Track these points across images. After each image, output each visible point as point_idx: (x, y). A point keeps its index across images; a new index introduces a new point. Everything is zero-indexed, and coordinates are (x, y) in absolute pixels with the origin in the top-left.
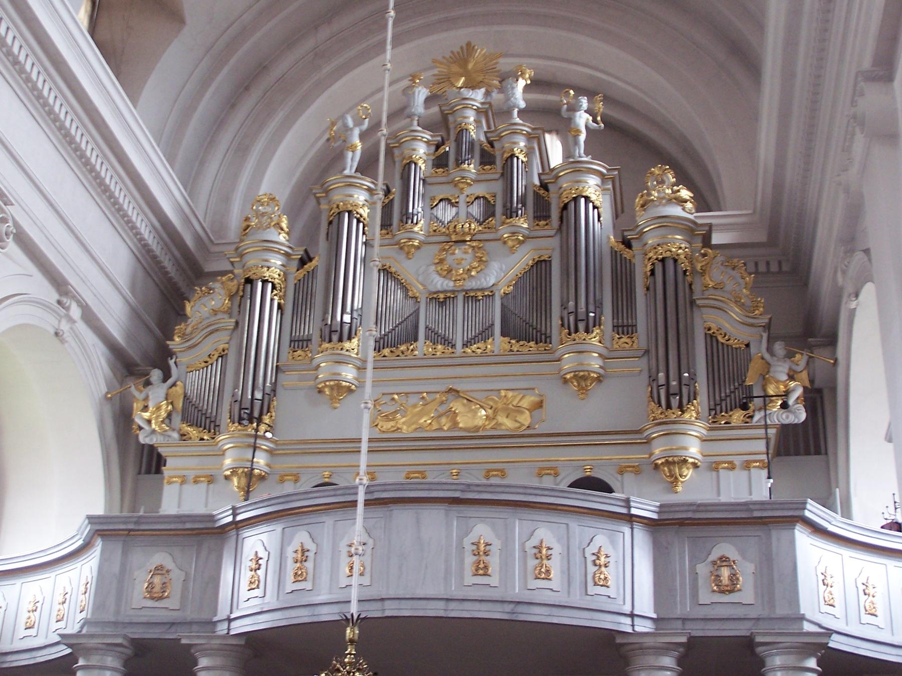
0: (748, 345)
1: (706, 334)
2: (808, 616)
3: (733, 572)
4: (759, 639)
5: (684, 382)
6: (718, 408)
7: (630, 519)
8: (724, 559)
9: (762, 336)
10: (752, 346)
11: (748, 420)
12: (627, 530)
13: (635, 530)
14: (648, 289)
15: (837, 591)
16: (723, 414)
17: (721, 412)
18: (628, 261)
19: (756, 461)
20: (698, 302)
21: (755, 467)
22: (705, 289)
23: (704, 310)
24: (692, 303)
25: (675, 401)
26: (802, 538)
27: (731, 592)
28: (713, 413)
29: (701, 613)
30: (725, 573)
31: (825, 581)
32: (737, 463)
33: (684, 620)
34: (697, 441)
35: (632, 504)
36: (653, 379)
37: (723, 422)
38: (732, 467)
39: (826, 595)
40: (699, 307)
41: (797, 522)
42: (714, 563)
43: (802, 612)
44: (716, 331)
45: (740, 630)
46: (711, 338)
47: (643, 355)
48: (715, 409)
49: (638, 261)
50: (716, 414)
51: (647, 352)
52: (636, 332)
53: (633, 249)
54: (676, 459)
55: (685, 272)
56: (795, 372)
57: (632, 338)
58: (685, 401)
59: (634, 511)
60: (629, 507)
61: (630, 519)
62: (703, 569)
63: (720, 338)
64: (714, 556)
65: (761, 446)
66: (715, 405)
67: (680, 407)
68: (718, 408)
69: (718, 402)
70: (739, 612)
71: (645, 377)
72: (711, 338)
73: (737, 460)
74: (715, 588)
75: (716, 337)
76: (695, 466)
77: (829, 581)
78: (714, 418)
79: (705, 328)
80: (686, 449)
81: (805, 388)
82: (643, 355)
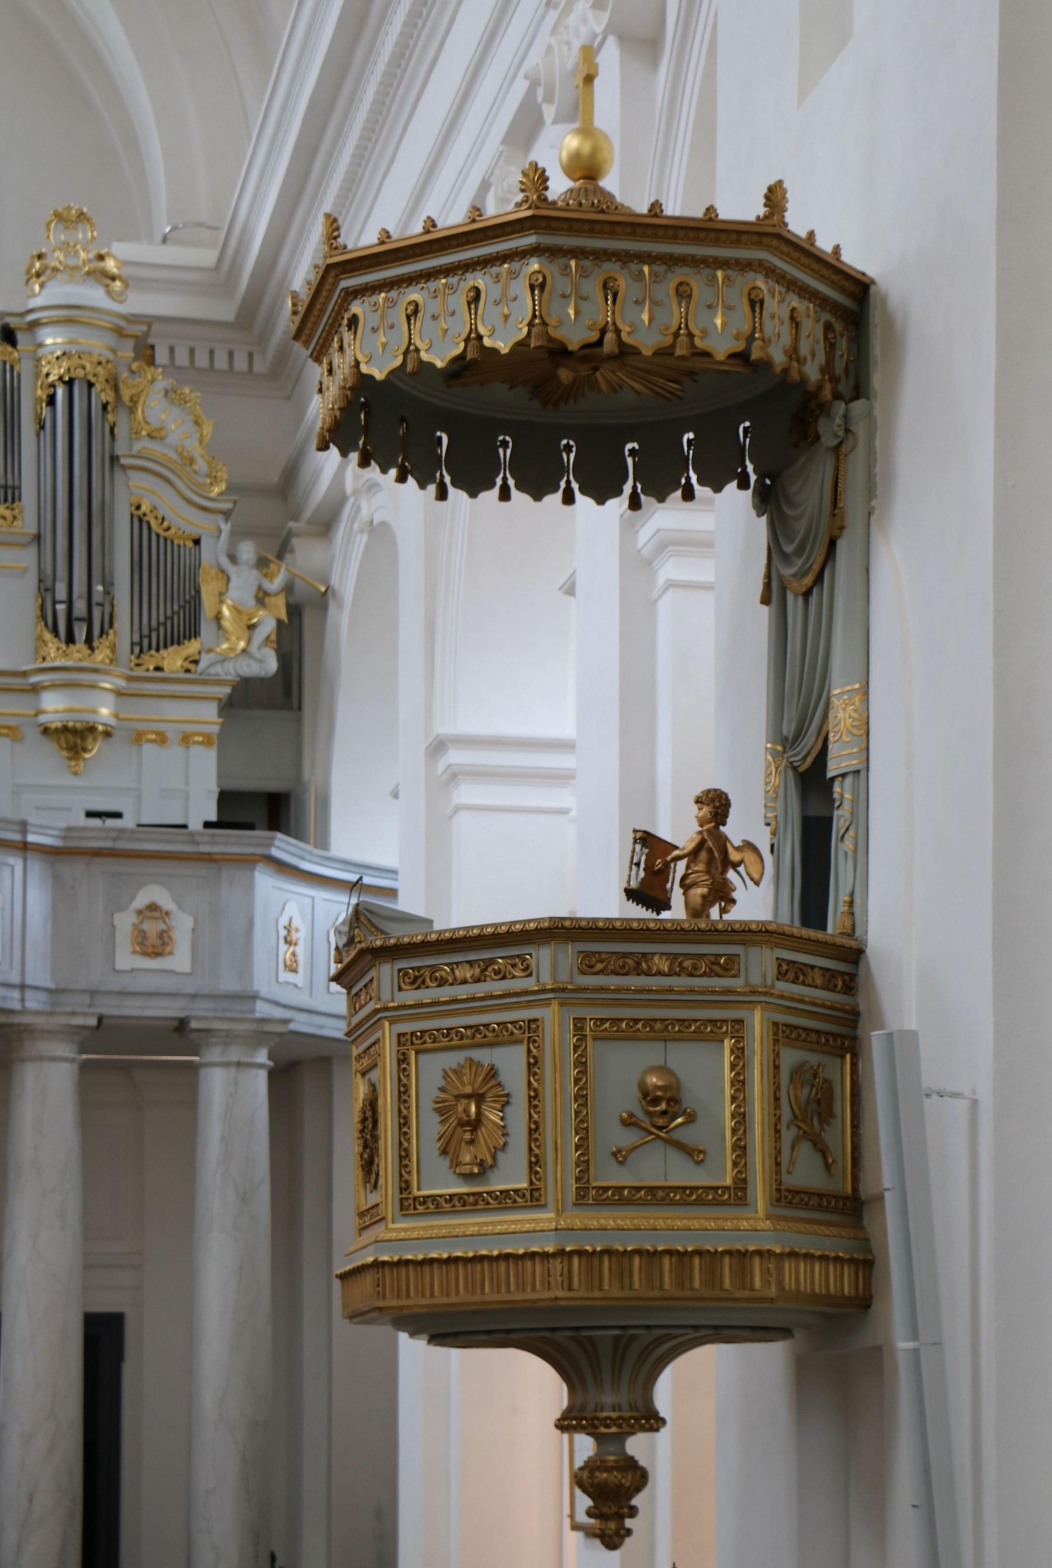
0: (197, 542)
1: (132, 516)
2: (264, 992)
3: (163, 926)
4: (194, 1025)
5: (97, 598)
6: (146, 642)
7: (24, 847)
8: (153, 907)
9: (220, 531)
10: (203, 541)
11: (192, 667)
12: (17, 863)
13: (29, 863)
14: (42, 427)
15: (300, 950)
16: (153, 652)
17: (150, 648)
18: (8, 367)
19: (199, 734)
20: (123, 461)
21: (198, 743)
22: (134, 436)
23: (132, 474)
24: (114, 459)
25: (80, 632)
26: (265, 882)
27: (157, 954)
28: (137, 649)
29: (116, 984)
30: (152, 928)
31: (289, 938)
32: (170, 735)
33: (93, 993)
34: (110, 698)
35: (30, 828)
36: (45, 589)
37: (152, 668)
38: (162, 739)
39: (288, 955)
40: (124, 468)
41: (259, 861)
42: (139, 912)
43: (256, 988)
44: (148, 512)
45: (172, 1009)
46: (139, 520)
47: (30, 543)
48: (141, 644)
49: (25, 369)
50: (141, 651)
51: (38, 538)
52: (20, 499)
53: (19, 347)
54: (78, 725)
55: (105, 407)
56: (267, 594)
57: (13, 509)
58: (96, 631)
59: (31, 838)
60: (24, 832)
61: (24, 847)
62: (125, 921)
63: (153, 523)
64: (141, 900)
65: (208, 714)
66: (141, 637)
67: (89, 641)
68: (146, 642)
69: (145, 631)
70: (169, 984)
71: (31, 581)
72: (139, 520)
73: (172, 732)
74: (137, 948)
75: (148, 523)
76: (107, 734)
77: (294, 936)
78: (138, 657)
79: (131, 505)
80: (94, 711)
81: (280, 622)
82: (30, 543)
